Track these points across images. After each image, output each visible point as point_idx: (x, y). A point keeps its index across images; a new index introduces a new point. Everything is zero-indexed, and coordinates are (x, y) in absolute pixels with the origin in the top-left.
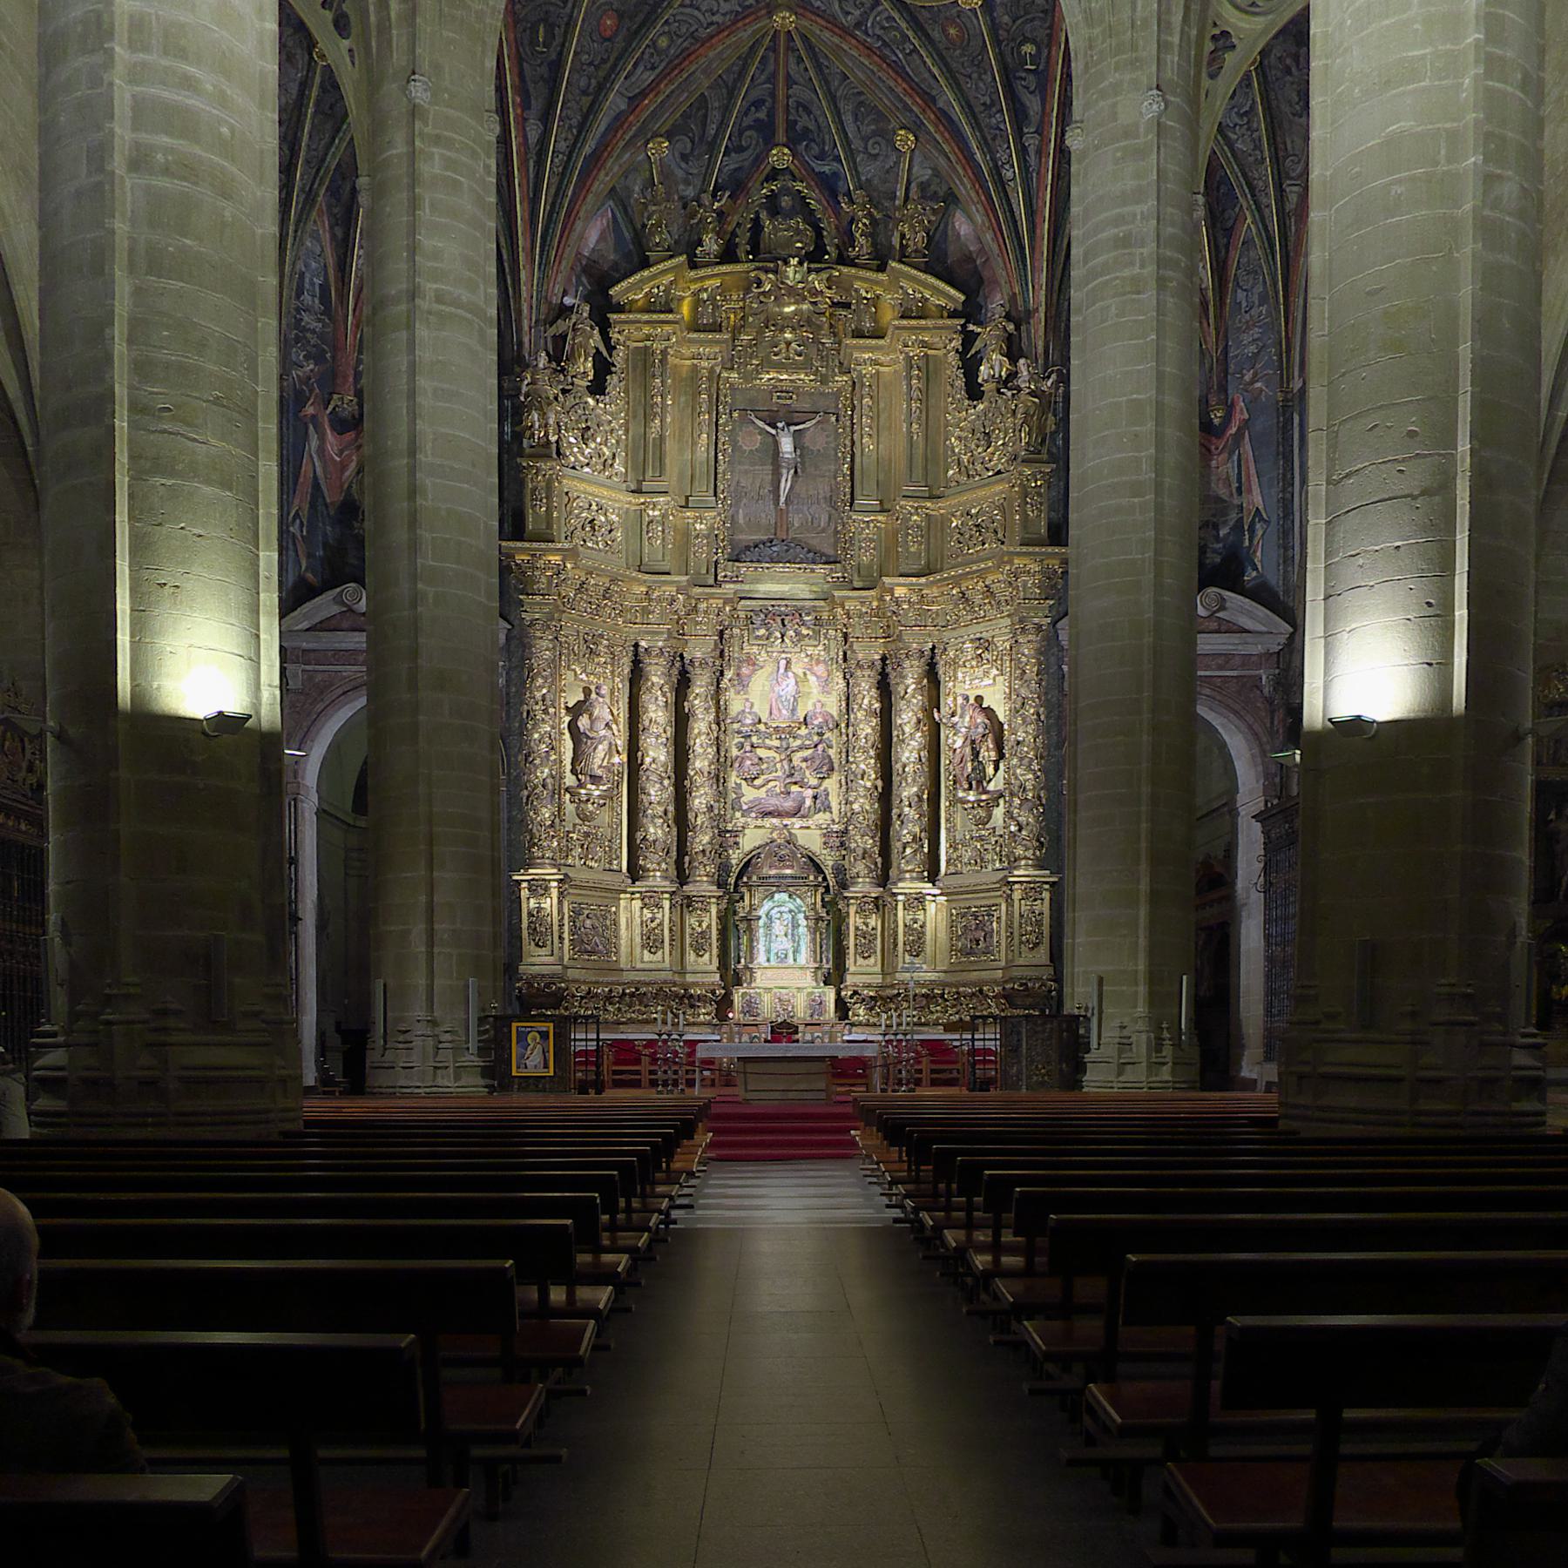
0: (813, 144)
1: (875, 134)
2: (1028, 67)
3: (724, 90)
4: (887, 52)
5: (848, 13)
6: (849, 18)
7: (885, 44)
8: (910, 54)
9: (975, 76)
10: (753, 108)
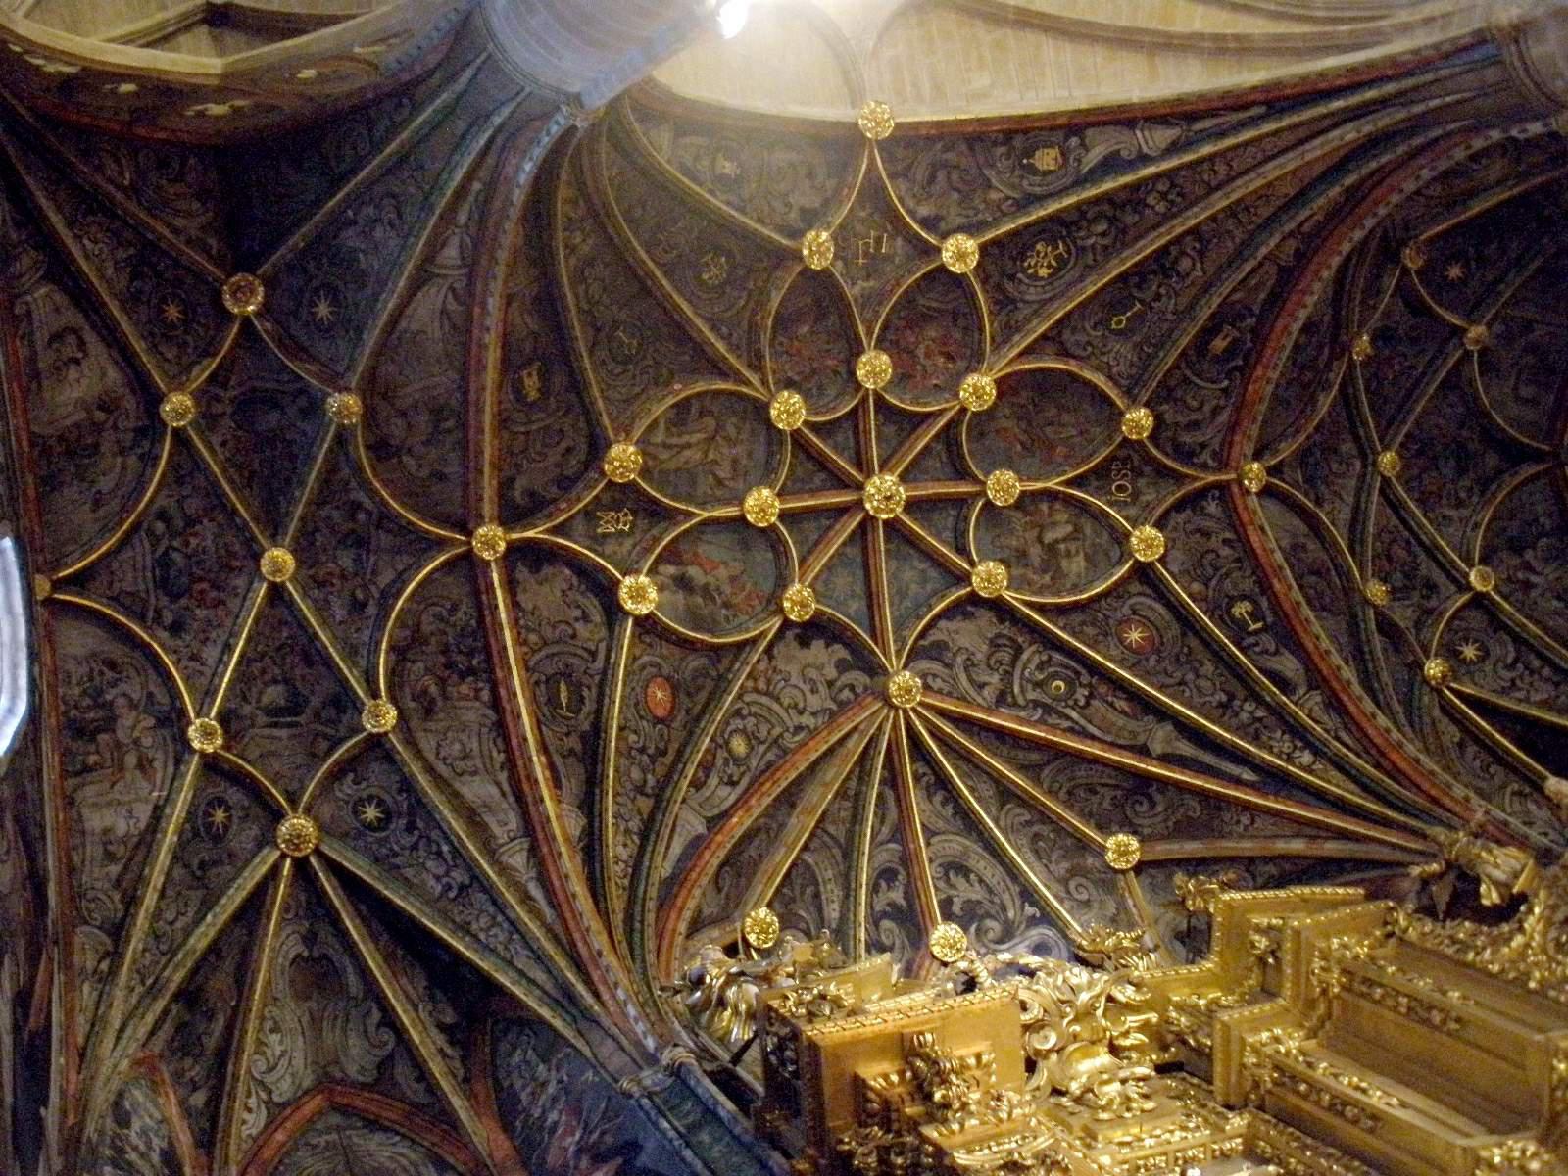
0: (989, 923)
1: (1073, 872)
2: (1253, 627)
3: (836, 851)
4: (1053, 720)
5: (981, 686)
6: (985, 692)
7: (1048, 710)
8: (1088, 704)
9: (1190, 677)
10: (883, 884)
